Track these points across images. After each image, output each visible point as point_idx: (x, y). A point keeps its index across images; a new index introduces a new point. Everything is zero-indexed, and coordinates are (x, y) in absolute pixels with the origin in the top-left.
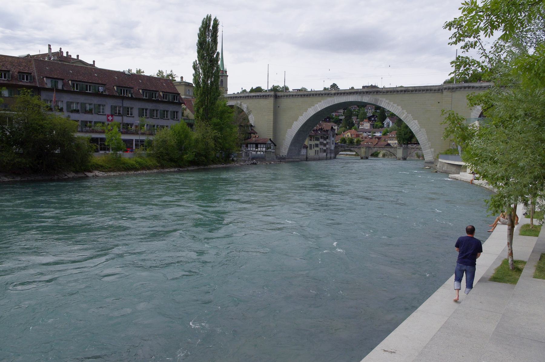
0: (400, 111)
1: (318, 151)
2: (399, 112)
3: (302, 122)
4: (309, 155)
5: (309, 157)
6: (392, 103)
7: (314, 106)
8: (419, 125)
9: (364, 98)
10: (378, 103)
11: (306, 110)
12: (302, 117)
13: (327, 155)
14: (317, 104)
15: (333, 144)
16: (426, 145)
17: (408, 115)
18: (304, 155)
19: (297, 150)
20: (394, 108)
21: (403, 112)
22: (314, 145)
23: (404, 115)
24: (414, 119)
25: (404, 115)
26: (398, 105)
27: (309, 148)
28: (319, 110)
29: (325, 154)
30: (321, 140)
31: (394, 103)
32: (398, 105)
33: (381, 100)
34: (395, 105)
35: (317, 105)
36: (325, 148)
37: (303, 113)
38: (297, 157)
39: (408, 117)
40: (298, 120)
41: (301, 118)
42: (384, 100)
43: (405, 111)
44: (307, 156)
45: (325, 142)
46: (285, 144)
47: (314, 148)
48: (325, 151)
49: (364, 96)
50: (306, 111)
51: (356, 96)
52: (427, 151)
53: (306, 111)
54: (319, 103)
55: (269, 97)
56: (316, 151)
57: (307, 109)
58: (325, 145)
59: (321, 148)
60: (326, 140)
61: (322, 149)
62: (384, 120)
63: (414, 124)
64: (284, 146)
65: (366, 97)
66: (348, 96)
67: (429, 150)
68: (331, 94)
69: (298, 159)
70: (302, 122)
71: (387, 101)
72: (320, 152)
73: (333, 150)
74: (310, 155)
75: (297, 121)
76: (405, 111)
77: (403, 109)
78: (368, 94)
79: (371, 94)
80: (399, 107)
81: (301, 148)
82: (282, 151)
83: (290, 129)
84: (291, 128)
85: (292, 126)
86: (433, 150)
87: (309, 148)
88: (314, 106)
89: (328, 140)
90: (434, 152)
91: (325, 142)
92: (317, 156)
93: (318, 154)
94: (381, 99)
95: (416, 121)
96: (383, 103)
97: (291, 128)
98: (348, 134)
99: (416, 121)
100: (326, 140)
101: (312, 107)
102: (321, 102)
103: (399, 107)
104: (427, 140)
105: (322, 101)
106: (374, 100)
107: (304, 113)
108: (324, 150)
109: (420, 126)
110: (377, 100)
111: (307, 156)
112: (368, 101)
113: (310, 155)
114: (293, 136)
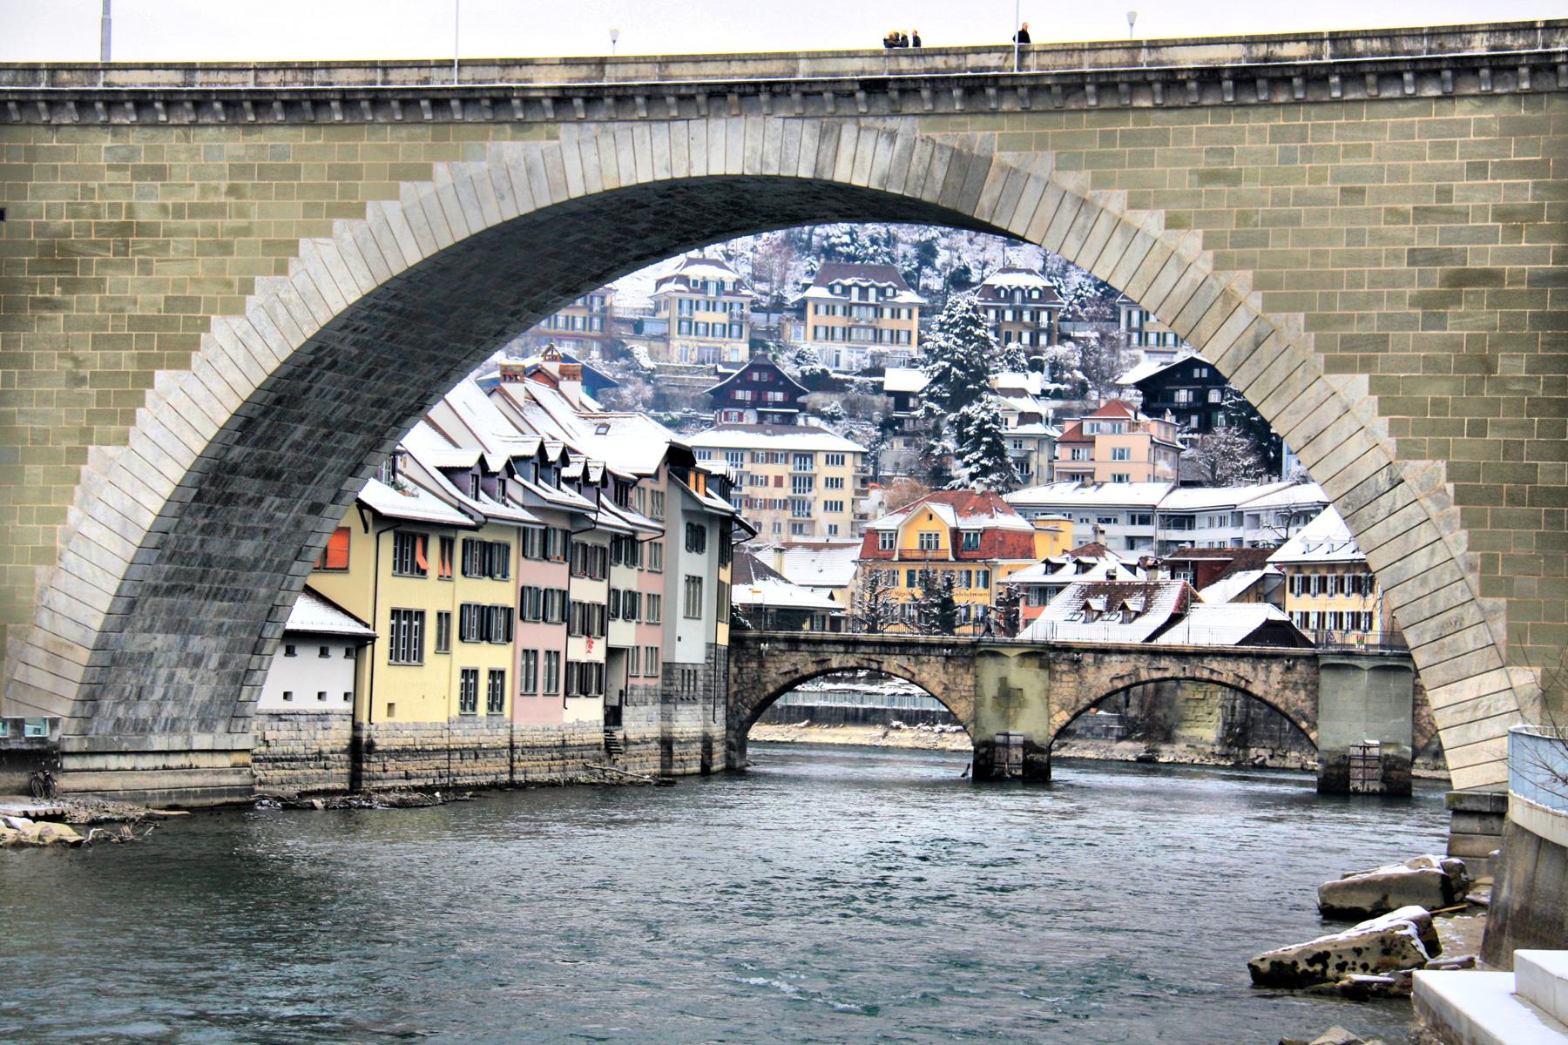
0: (1195, 275)
2: (1185, 286)
3: (234, 376)
4: (380, 715)
5: (382, 743)
7: (359, 212)
9: (846, 149)
10: (985, 200)
11: (281, 253)
12: (235, 321)
13: (613, 716)
14: (394, 195)
16: (1459, 627)
17: (1277, 318)
18: (323, 716)
19: (213, 663)
20: (1139, 247)
21: (1226, 294)
22: (443, 617)
23: (1240, 321)
24: (1334, 366)
25: (1240, 321)
26: (1173, 223)
27: (383, 646)
28: (413, 257)
29: (587, 712)
30: (551, 575)
31: (1135, 204)
32: (1173, 223)
33: (1011, 172)
34: (1151, 221)
35: (392, 208)
37: (248, 287)
38: (202, 741)
39: (1268, 348)
40: (196, 358)
41: (222, 332)
42: (1042, 164)
43: (1239, 281)
44: (356, 727)
45: (588, 591)
46: (60, 602)
47: (443, 645)
48: (583, 680)
49: (848, 131)
50: (282, 269)
51: (775, 124)
52: (1468, 689)
53: (282, 269)
54: (405, 186)
56: (469, 675)
57: (292, 247)
58: (588, 621)
59: (530, 654)
60: (605, 575)
61: (552, 655)
63: (1333, 409)
64: (45, 617)
65: (868, 139)
66: (698, 126)
67: (1495, 680)
68: (529, 102)
69: (224, 761)
70: (234, 376)
71: (1074, 181)
72: (529, 687)
73: (689, 673)
74: (400, 717)
75: (183, 363)
76: (1239, 281)
77: (1221, 263)
78: (882, 105)
79: (911, 108)
80: (1190, 243)
81: (256, 650)
82: (20, 673)
83: (110, 450)
84: (124, 440)
85: (130, 419)
87: (383, 646)
88: (359, 212)
89: (624, 577)
91: (588, 591)
93: (496, 702)
94: (1008, 158)
95: (1356, 385)
96: (1031, 192)
97: (124, 440)
99: (1356, 385)
100: (605, 575)
101: (338, 224)
102: (425, 174)
103: (1190, 243)
104: (1473, 578)
105: (440, 169)
106: (940, 172)
107: (260, 281)
109: (1394, 429)
111: (356, 727)
112: (886, 178)
113: (400, 717)
114: (148, 520)
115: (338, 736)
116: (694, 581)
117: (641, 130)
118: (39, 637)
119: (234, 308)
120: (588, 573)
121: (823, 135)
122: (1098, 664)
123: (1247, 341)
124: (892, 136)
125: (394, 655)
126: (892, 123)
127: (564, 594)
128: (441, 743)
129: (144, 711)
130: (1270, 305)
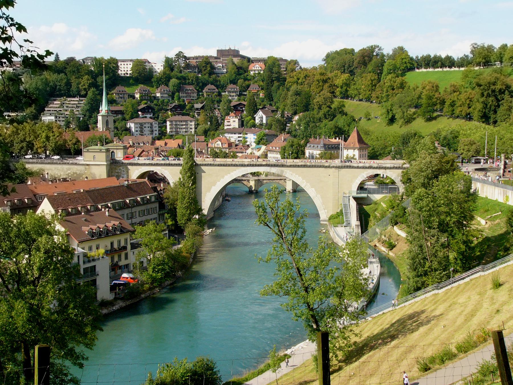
6: (294, 174)
8: (315, 192)
11: (223, 177)
23: (304, 184)
25: (304, 184)
34: (297, 176)
35: (233, 173)
41: (218, 183)
42: (288, 171)
62: (255, 112)
71: (291, 173)
76: (304, 181)
80: (300, 178)
86: (326, 211)
90: (328, 212)
94: (285, 171)
95: (313, 189)
98: (218, 143)
99: (313, 189)
110: (282, 171)
119: (219, 181)
130: (307, 183)
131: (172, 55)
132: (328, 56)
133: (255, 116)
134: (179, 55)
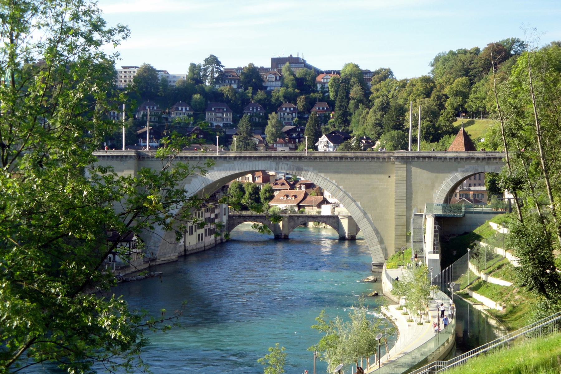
1: (202, 234)
4: (188, 245)
15: (225, 214)
27: (188, 233)
29: (213, 237)
36: (212, 226)
44: (185, 247)
47: (196, 231)
48: (213, 232)
52: (375, 248)
53: (190, 183)
55: (128, 159)
56: (199, 235)
64: (153, 238)
65: (284, 165)
72: (206, 235)
78: (286, 160)
87: (188, 233)
91: (213, 216)
92: (201, 245)
93: (202, 239)
108: (212, 230)
115: (183, 248)
116: (225, 209)
117: (248, 163)
118: (152, 241)
120: (212, 213)
121: (277, 164)
122: (298, 219)
123: (342, 197)
124: (287, 164)
125: (190, 234)
126: (288, 162)
127: (210, 218)
128: (196, 248)
129: (165, 251)
131: (200, 61)
132: (437, 59)
133: (317, 144)
134: (213, 61)
